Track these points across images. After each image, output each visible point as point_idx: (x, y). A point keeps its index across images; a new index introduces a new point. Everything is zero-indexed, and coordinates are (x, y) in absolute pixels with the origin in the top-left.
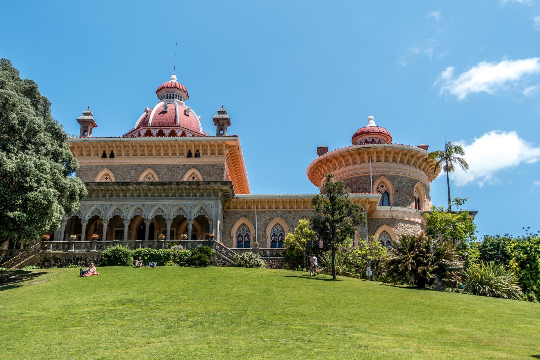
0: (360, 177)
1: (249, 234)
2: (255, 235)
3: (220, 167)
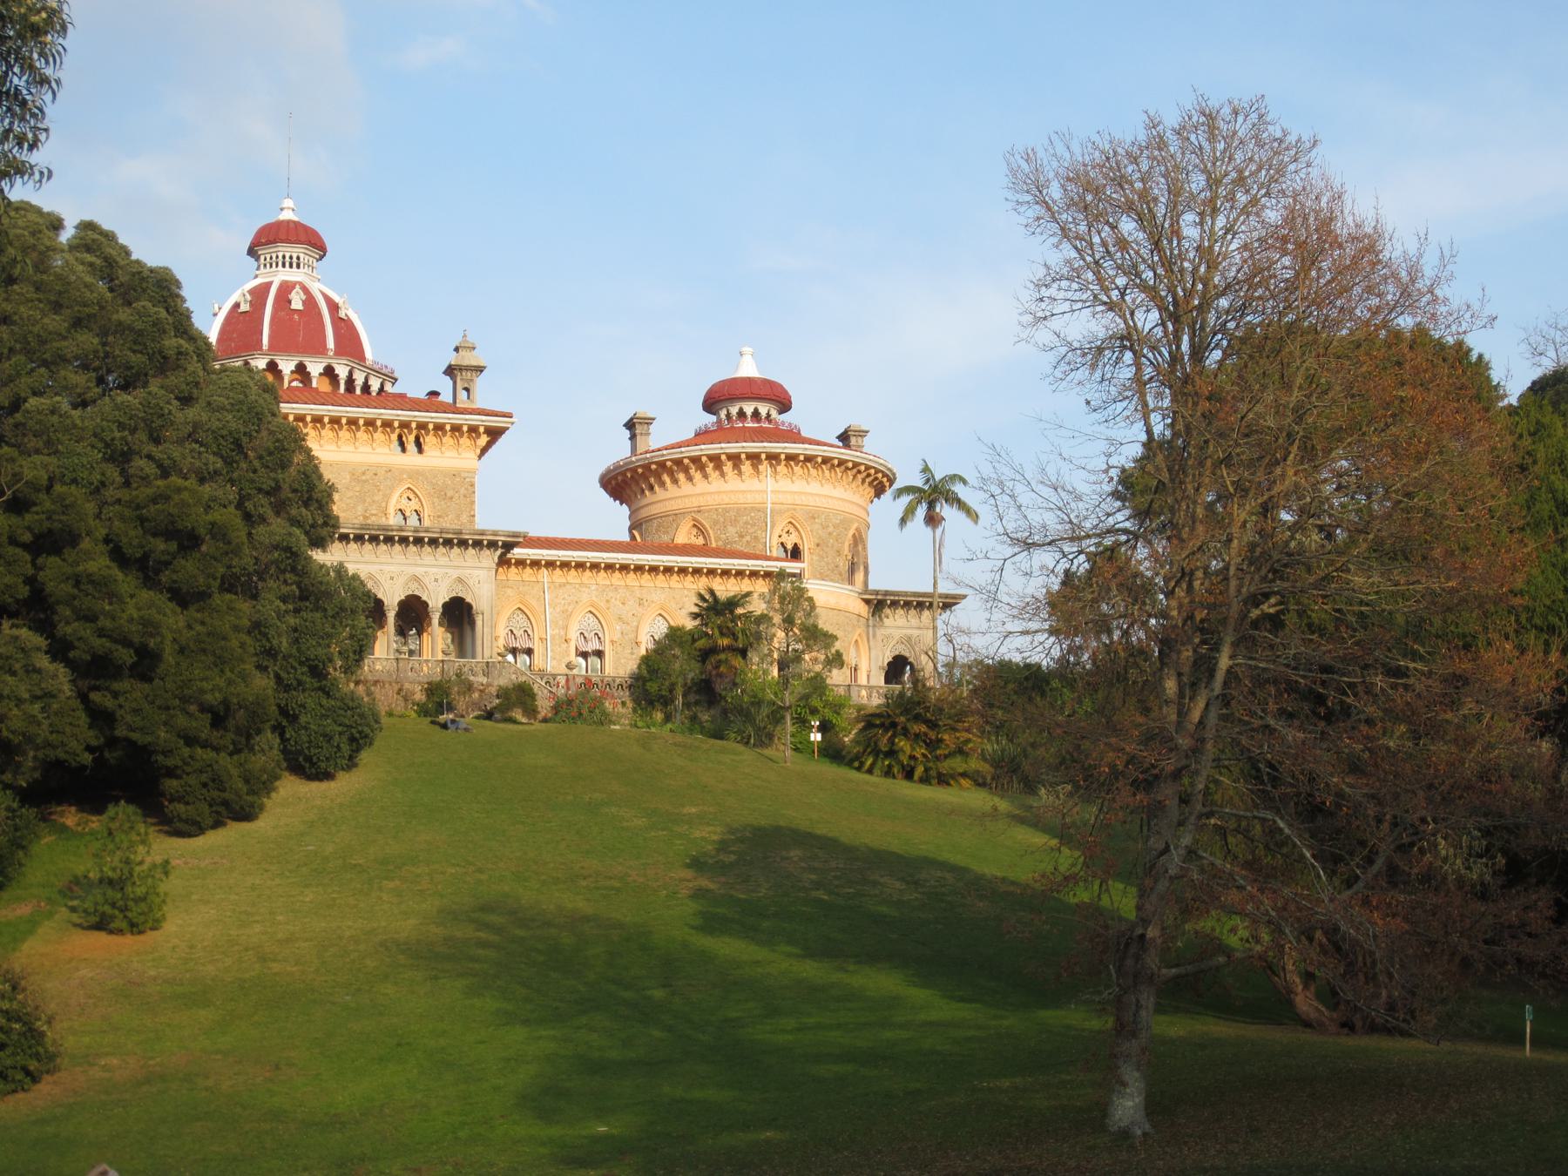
0: (745, 509)
1: (530, 632)
2: (544, 636)
3: (468, 480)
